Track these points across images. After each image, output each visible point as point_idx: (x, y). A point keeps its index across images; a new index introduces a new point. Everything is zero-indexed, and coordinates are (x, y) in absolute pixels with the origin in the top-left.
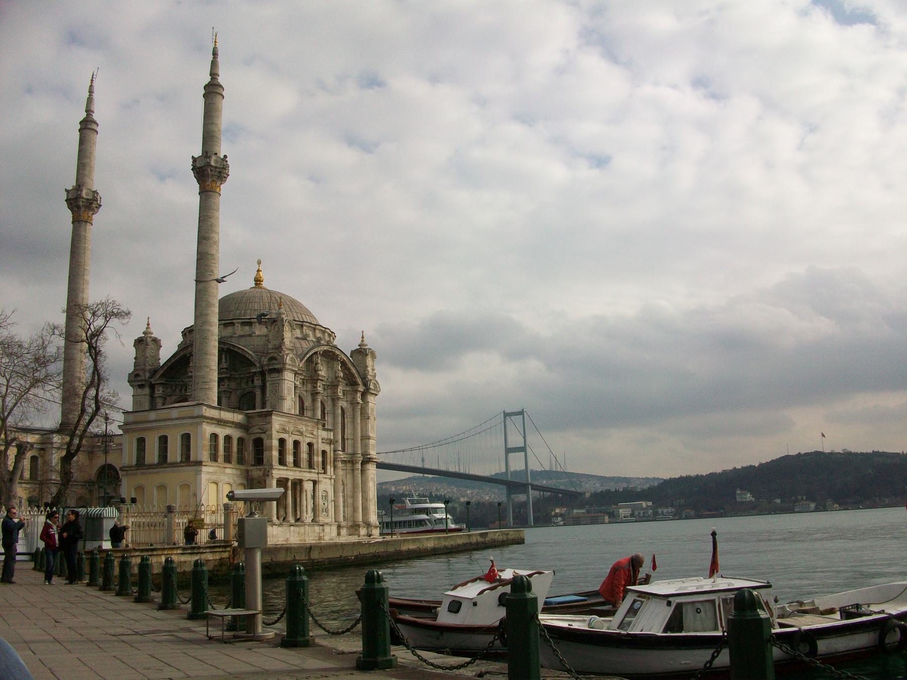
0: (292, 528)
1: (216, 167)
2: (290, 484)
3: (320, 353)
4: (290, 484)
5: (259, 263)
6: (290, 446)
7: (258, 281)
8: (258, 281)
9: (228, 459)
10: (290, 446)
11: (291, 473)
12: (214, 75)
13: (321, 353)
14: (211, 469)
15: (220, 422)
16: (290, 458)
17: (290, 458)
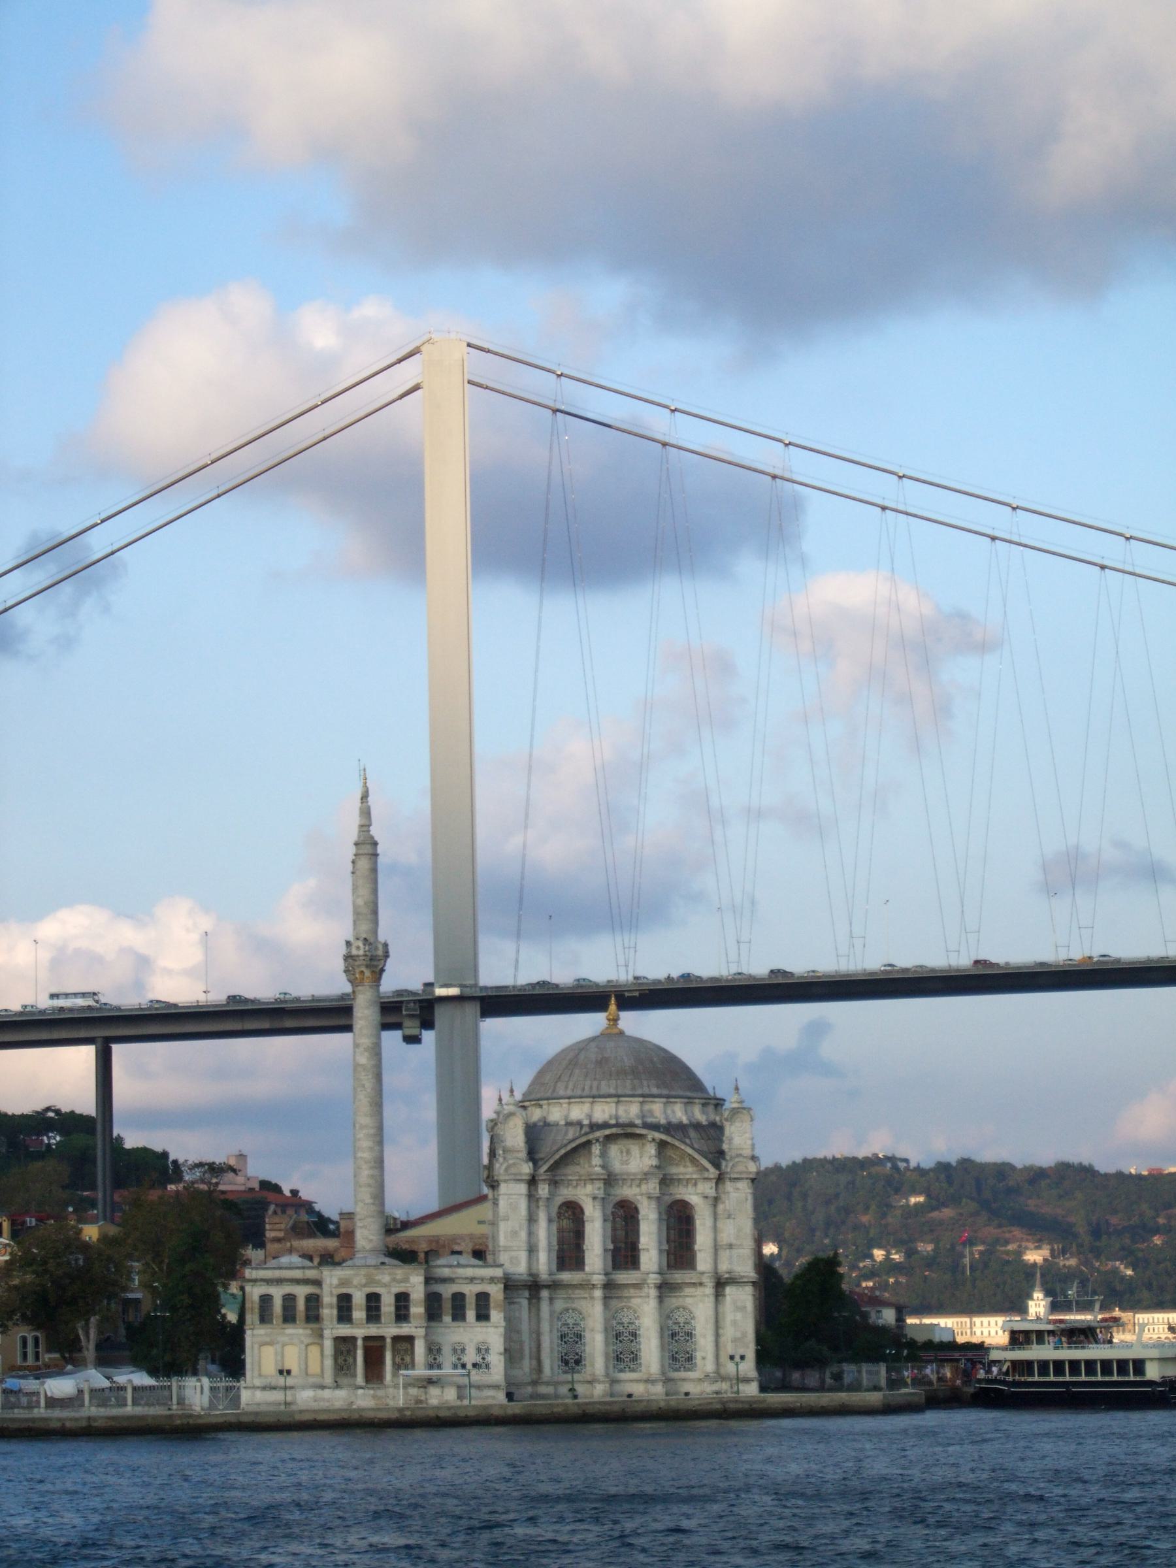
0: (360, 1391)
1: (358, 956)
2: (360, 1343)
4: (360, 1343)
6: (359, 1298)
9: (289, 1317)
10: (359, 1298)
11: (363, 1331)
12: (365, 827)
13: (601, 1140)
14: (262, 1332)
15: (269, 1282)
16: (359, 1314)
17: (359, 1314)
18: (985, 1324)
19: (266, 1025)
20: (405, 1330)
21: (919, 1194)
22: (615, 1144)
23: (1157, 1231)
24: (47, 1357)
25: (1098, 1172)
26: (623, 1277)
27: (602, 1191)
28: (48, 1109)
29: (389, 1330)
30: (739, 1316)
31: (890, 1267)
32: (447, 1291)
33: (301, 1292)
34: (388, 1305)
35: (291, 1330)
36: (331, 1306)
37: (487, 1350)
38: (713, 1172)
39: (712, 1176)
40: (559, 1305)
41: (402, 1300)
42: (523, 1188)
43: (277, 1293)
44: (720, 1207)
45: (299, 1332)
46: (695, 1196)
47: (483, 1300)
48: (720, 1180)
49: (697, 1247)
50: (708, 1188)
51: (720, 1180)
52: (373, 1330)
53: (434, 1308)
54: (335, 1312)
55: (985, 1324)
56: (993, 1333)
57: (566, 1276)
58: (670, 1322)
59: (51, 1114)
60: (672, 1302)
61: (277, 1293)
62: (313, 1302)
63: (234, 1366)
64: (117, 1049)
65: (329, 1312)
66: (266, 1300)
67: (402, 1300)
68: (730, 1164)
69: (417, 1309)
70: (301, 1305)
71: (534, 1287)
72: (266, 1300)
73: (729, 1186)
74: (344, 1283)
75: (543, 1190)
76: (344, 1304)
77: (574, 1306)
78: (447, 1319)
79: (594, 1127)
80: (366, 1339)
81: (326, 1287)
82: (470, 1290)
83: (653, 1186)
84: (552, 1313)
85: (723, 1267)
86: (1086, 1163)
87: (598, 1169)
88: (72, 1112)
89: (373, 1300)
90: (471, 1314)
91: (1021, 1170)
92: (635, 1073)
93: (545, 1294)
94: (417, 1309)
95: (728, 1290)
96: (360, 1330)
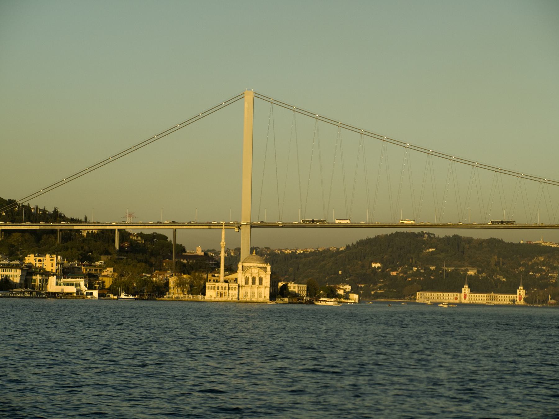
9: (211, 289)
10: (220, 287)
15: (209, 284)
16: (220, 289)
18: (447, 295)
20: (225, 291)
21: (433, 248)
23: (521, 265)
24: (180, 292)
25: (504, 242)
26: (253, 286)
28: (154, 233)
29: (224, 291)
31: (418, 273)
32: (231, 286)
33: (213, 286)
34: (224, 288)
35: (211, 290)
38: (265, 273)
41: (225, 287)
43: (210, 286)
44: (266, 278)
45: (213, 290)
46: (262, 276)
47: (235, 287)
50: (264, 275)
51: (266, 274)
52: (222, 291)
53: (229, 289)
55: (447, 295)
56: (450, 298)
57: (246, 285)
59: (155, 234)
60: (259, 289)
62: (214, 287)
63: (204, 294)
65: (216, 288)
66: (209, 286)
67: (225, 287)
70: (213, 287)
72: (209, 286)
74: (219, 285)
75: (244, 274)
76: (218, 288)
78: (231, 290)
79: (250, 267)
83: (257, 274)
85: (266, 285)
86: (500, 238)
88: (160, 234)
89: (222, 287)
90: (234, 290)
91: (476, 240)
92: (256, 260)
94: (227, 289)
95: (266, 288)
96: (220, 291)
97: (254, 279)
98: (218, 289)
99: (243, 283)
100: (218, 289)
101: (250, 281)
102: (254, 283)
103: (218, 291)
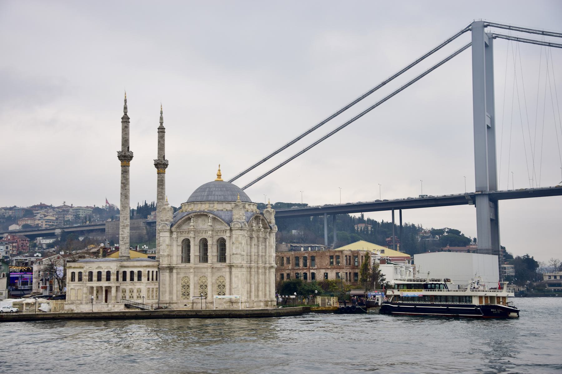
3: (192, 217)
5: (219, 166)
7: (219, 176)
8: (219, 176)
15: (74, 268)
16: (95, 278)
17: (95, 278)
19: (434, 203)
22: (201, 218)
27: (193, 235)
29: (104, 284)
30: (236, 279)
34: (104, 276)
36: (86, 275)
37: (140, 292)
38: (229, 228)
39: (228, 229)
40: (182, 275)
41: (108, 273)
42: (168, 234)
43: (77, 271)
48: (231, 230)
49: (226, 254)
50: (228, 234)
51: (231, 230)
54: (87, 278)
58: (218, 281)
61: (77, 271)
64: (403, 210)
65: (85, 277)
67: (108, 273)
68: (233, 224)
69: (113, 277)
71: (171, 269)
73: (234, 232)
75: (175, 235)
77: (187, 275)
80: (97, 287)
81: (85, 269)
82: (136, 270)
84: (177, 278)
87: (192, 227)
89: (99, 273)
90: (136, 278)
93: (175, 271)
95: (233, 269)
96: (95, 284)
97: (204, 244)
98: (91, 279)
99: (176, 260)
100: (91, 279)
101: (195, 251)
102: (204, 258)
103: (90, 284)
